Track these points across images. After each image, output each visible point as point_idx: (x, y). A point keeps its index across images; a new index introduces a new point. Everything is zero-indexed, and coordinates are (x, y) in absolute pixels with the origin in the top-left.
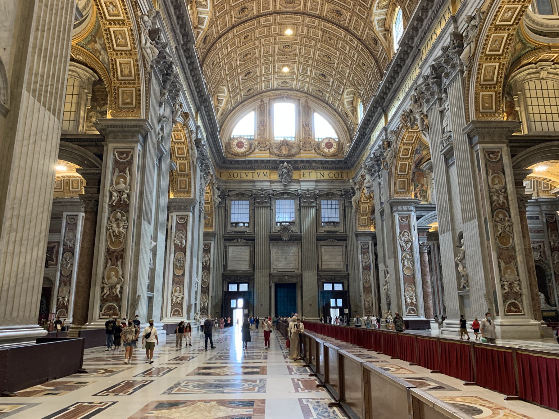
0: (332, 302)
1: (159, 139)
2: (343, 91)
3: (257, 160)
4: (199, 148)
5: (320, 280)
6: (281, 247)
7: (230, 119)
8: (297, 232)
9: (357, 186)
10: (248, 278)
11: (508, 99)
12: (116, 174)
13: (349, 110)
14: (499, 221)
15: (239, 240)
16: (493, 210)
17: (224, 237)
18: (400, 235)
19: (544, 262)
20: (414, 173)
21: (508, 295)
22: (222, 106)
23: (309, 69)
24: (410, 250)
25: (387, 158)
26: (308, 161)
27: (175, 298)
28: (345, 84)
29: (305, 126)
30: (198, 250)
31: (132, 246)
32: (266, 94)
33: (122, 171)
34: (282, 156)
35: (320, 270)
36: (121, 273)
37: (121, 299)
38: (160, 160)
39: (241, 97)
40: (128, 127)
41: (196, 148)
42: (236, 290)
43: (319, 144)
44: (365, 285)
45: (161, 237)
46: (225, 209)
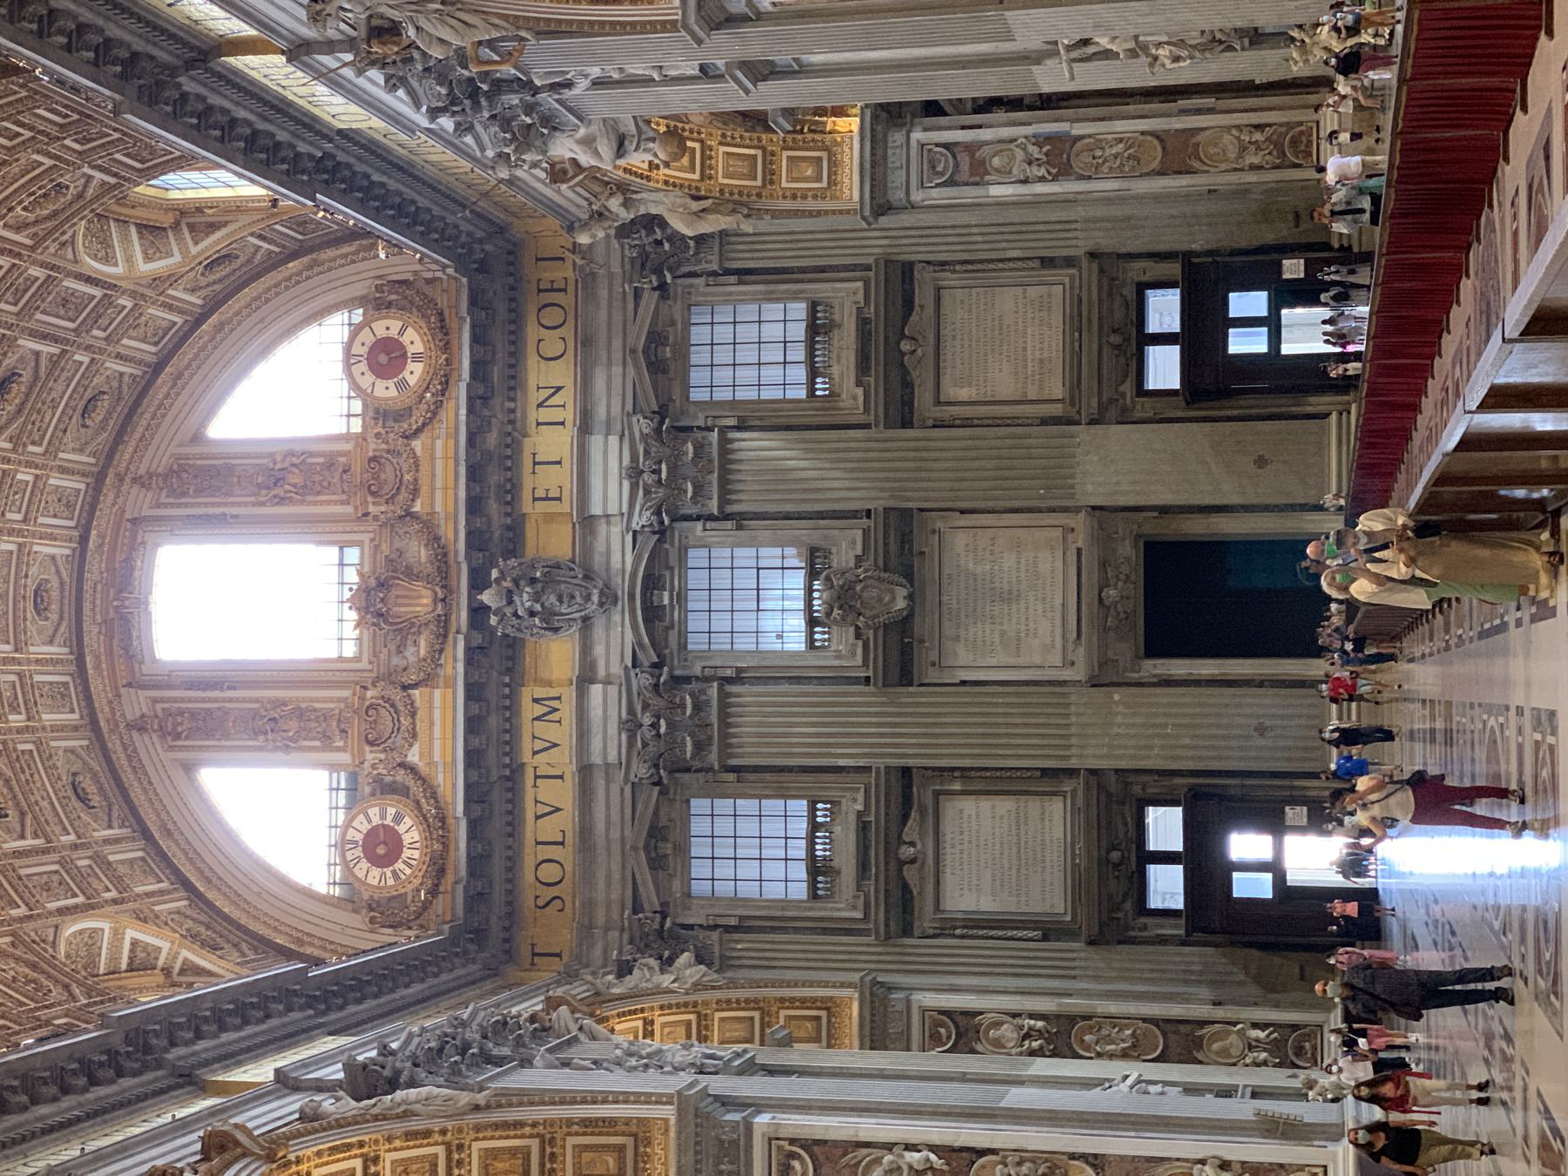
0: (1245, 343)
2: (89, 280)
4: (397, 1073)
5: (1124, 410)
6: (946, 624)
7: (237, 899)
8: (866, 532)
9: (614, 204)
13: (194, 250)
15: (907, 852)
17: (888, 937)
22: (165, 946)
26: (475, 473)
28: (53, 268)
29: (278, 491)
30: (963, 1078)
32: (101, 703)
35: (1072, 412)
39: (117, 841)
41: (400, 1095)
42: (1180, 868)
43: (379, 414)
44: (1155, 165)
46: (736, 929)
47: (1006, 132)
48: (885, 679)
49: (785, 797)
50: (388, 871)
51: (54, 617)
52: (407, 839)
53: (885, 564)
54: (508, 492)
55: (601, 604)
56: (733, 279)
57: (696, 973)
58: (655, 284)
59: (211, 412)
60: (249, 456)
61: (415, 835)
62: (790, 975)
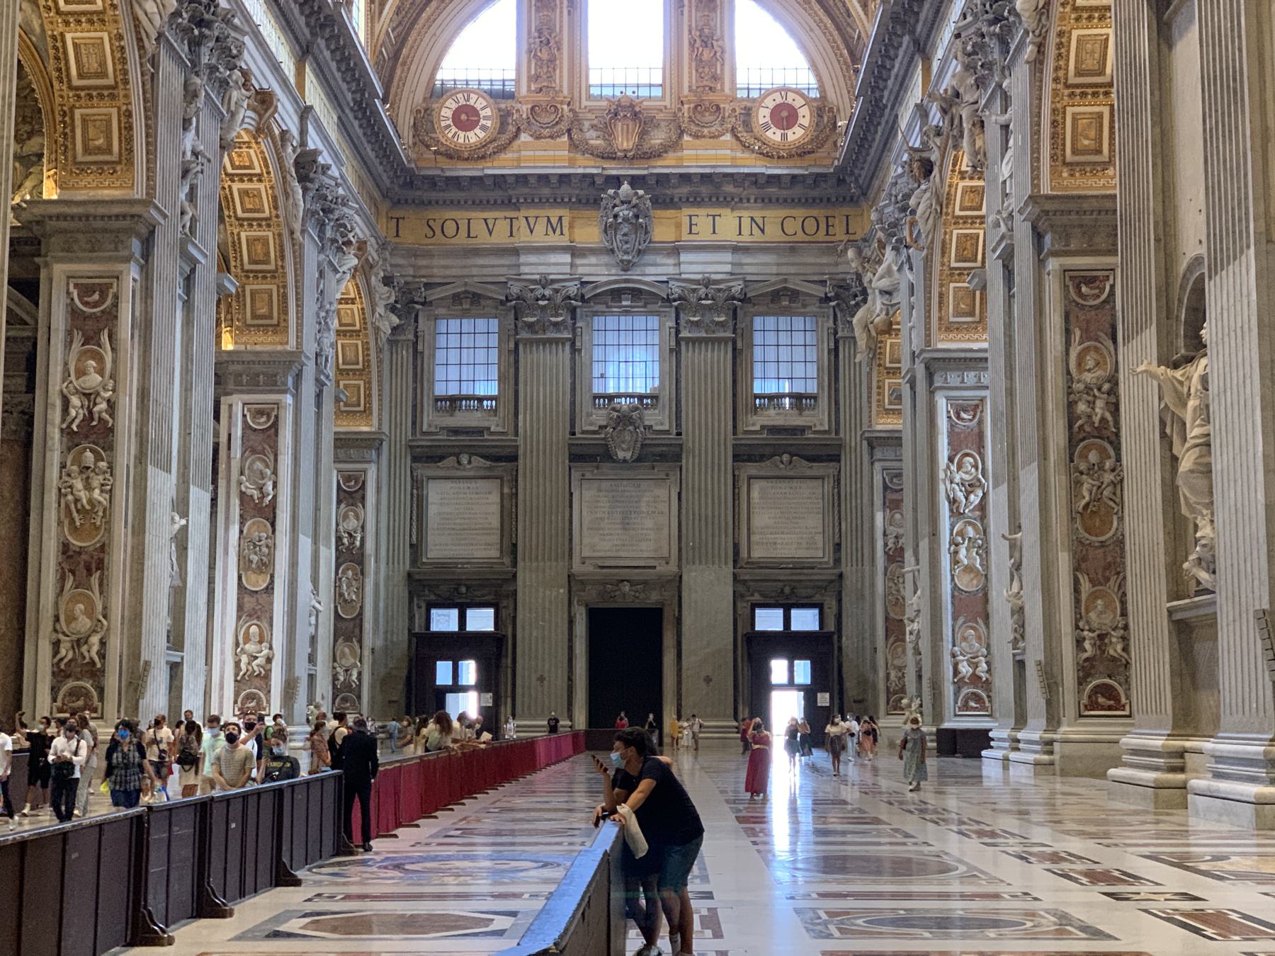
0: (778, 669)
1: (184, 227)
3: (525, 176)
4: (311, 181)
5: (742, 596)
6: (609, 483)
7: (431, 21)
12: (77, 346)
14: (1085, 471)
16: (1073, 440)
18: (948, 467)
21: (1093, 667)
24: (978, 513)
25: (919, 212)
27: (244, 659)
31: (126, 535)
33: (91, 338)
35: (741, 563)
36: (99, 607)
37: (103, 671)
38: (189, 281)
40: (102, 217)
42: (456, 629)
44: (892, 615)
45: (199, 497)
48: (573, 445)
49: (499, 380)
50: (450, 122)
52: (471, 134)
53: (646, 445)
54: (695, 199)
55: (622, 261)
56: (832, 345)
57: (386, 328)
58: (829, 295)
62: (386, 387)
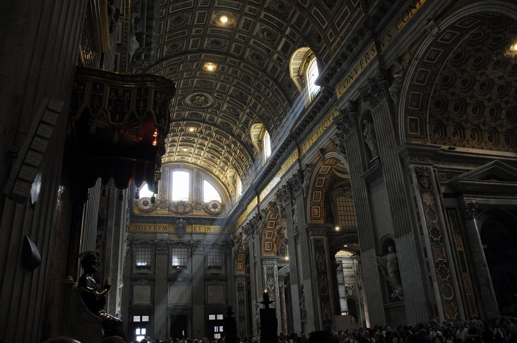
0: (216, 329)
3: (159, 217)
10: (149, 311)
11: (328, 207)
13: (230, 182)
15: (143, 280)
16: (319, 273)
19: (355, 297)
20: (276, 238)
23: (203, 152)
24: (273, 291)
25: (259, 227)
28: (229, 166)
29: (197, 190)
34: (179, 214)
43: (207, 205)
47: (245, 294)
51: (180, 159)
52: (146, 207)
55: (180, 236)
56: (225, 255)
59: (207, 181)
60: (201, 186)
61: (147, 208)
